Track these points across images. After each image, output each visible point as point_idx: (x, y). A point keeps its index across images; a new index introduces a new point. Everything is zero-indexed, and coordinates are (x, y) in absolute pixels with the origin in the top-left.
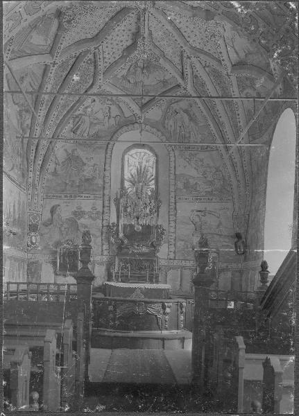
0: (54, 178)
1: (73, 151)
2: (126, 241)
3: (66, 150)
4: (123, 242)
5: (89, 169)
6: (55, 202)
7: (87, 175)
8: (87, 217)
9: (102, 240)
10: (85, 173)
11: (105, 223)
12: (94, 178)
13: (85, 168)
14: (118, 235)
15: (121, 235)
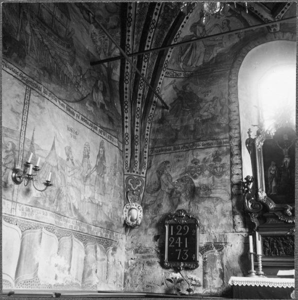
0: (161, 125)
2: (272, 206)
4: (265, 207)
6: (163, 158)
8: (207, 173)
9: (233, 208)
11: (235, 179)
12: (214, 118)
13: (201, 105)
14: (257, 195)
15: (262, 195)
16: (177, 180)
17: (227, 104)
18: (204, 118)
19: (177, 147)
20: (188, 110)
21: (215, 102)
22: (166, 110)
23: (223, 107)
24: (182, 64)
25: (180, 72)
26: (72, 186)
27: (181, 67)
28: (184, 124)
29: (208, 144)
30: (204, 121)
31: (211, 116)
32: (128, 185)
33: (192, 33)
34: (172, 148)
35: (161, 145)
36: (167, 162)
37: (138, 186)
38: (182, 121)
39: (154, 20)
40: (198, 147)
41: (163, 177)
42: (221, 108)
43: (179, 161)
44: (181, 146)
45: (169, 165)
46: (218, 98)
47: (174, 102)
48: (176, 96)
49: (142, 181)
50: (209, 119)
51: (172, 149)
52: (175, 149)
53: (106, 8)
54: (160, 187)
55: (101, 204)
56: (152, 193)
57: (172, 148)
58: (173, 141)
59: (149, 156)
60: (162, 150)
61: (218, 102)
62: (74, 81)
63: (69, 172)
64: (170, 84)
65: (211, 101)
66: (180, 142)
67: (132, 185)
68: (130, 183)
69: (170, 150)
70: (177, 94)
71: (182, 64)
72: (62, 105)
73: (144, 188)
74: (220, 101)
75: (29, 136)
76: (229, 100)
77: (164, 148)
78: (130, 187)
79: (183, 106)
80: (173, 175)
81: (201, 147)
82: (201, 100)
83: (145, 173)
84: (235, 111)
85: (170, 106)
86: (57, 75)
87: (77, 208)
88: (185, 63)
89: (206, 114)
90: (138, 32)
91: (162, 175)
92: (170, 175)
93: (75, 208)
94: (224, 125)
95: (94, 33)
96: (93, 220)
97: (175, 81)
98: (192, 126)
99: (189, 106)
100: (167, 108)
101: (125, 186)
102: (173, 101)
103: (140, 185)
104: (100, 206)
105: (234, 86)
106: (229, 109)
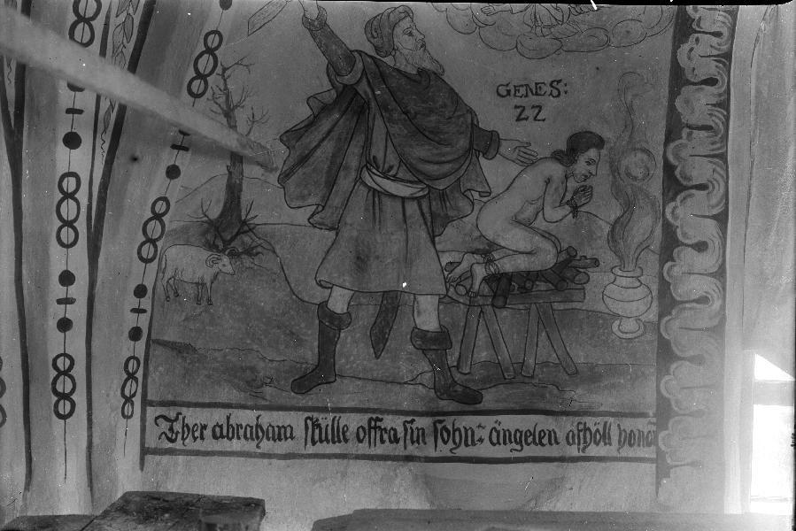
5: (531, 182)
7: (516, 239)
10: (494, 222)
13: (494, 171)
17: (656, 187)
18: (507, 265)
19: (325, 420)
21: (581, 166)
23: (629, 206)
28: (376, 284)
29: (521, 438)
30: (505, 287)
31: (547, 258)
34: (296, 420)
40: (463, 451)
42: (615, 212)
44: (353, 422)
46: (600, 143)
47: (311, 123)
50: (538, 275)
51: (299, 432)
61: (604, 170)
65: (557, 156)
66: (346, 393)
69: (281, 434)
70: (333, 70)
74: (614, 170)
76: (669, 169)
77: (246, 417)
79: (369, 163)
81: (485, 450)
82: (487, 143)
84: (701, 247)
85: (282, 149)
89: (516, 239)
94: (630, 325)
98: (428, 304)
99: (412, 169)
102: (304, 112)
105: (711, 82)
106: (669, 230)
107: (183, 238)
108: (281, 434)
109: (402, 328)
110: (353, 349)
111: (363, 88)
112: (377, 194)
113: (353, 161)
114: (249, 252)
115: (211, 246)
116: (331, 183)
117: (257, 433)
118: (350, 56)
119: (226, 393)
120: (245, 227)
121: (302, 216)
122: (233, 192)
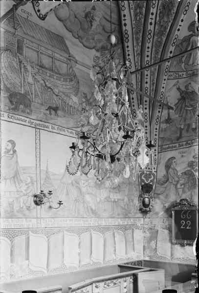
0: (168, 125)
1: (186, 87)
3: (179, 89)
16: (182, 173)
20: (190, 109)
22: (171, 111)
24: (184, 64)
25: (183, 73)
26: (88, 193)
27: (184, 68)
32: (141, 180)
33: (191, 33)
34: (177, 145)
35: (168, 143)
36: (173, 158)
37: (150, 179)
38: (185, 121)
39: (150, 30)
41: (170, 170)
43: (182, 156)
44: (184, 143)
45: (175, 160)
47: (179, 101)
48: (180, 97)
49: (154, 175)
52: (180, 146)
53: (105, 31)
54: (168, 180)
55: (116, 200)
56: (162, 184)
57: (177, 145)
58: (178, 139)
59: (158, 153)
60: (169, 148)
62: (80, 109)
63: (84, 184)
64: (174, 85)
66: (183, 139)
67: (145, 179)
68: (143, 178)
69: (175, 147)
70: (181, 94)
71: (184, 64)
72: (71, 133)
73: (155, 180)
75: (43, 167)
77: (171, 145)
78: (144, 181)
79: (186, 106)
80: (178, 169)
83: (156, 168)
85: (174, 107)
86: (63, 110)
87: (94, 208)
88: (187, 64)
90: (138, 43)
91: (169, 169)
92: (176, 170)
93: (92, 209)
95: (96, 57)
96: (110, 214)
97: (178, 82)
100: (172, 108)
101: (140, 180)
102: (177, 101)
103: (152, 179)
104: (116, 202)
107: (163, 123)
108: (175, 147)
109: (191, 128)
110: (184, 133)
111: (185, 96)
112: (187, 110)
113: (184, 106)
114: (171, 122)
115: (166, 123)
116: (181, 110)
117: (172, 147)
118: (183, 92)
119: (168, 143)
120: (171, 119)
121: (177, 116)
122: (169, 114)
